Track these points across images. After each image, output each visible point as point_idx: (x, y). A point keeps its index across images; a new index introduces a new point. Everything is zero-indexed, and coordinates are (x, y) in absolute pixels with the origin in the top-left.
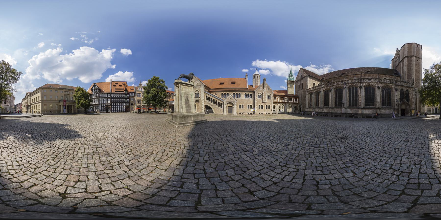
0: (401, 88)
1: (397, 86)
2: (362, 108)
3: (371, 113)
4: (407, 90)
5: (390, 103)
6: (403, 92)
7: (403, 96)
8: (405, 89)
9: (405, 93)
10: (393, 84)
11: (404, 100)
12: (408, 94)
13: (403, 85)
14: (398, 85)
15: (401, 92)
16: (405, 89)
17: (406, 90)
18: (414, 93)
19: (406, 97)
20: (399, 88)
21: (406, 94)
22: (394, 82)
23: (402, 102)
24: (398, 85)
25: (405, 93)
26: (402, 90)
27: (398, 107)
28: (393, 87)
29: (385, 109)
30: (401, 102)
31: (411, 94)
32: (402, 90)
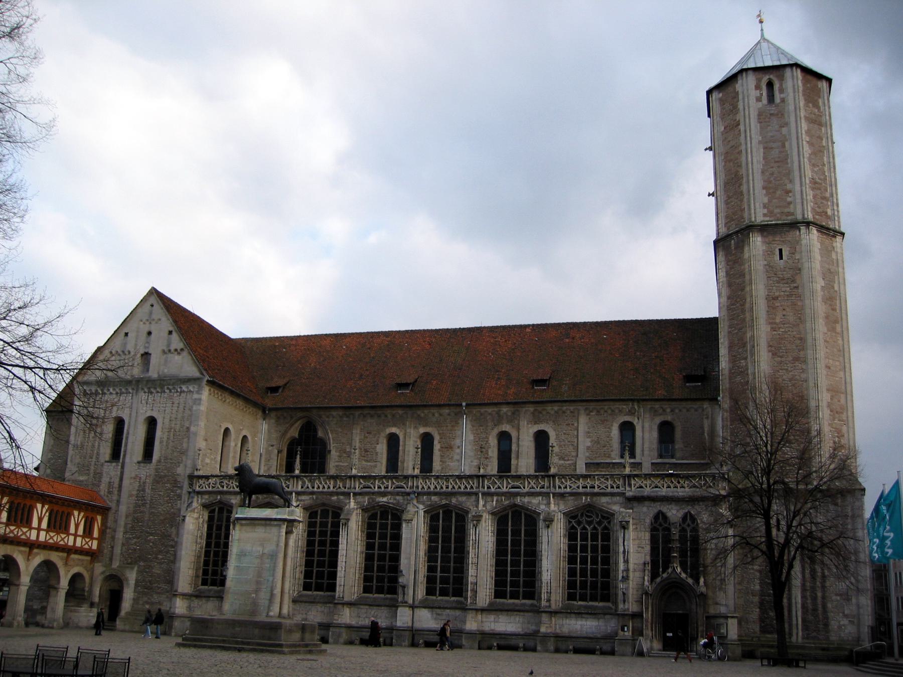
1: (635, 504)
2: (483, 610)
3: (520, 630)
4: (689, 518)
5: (606, 586)
6: (669, 530)
7: (668, 551)
8: (674, 513)
9: (675, 531)
10: (612, 495)
11: (670, 570)
15: (653, 529)
17: (684, 518)
19: (683, 554)
21: (683, 539)
22: (620, 483)
23: (658, 580)
26: (660, 517)
28: (616, 508)
29: (579, 614)
32: (660, 517)
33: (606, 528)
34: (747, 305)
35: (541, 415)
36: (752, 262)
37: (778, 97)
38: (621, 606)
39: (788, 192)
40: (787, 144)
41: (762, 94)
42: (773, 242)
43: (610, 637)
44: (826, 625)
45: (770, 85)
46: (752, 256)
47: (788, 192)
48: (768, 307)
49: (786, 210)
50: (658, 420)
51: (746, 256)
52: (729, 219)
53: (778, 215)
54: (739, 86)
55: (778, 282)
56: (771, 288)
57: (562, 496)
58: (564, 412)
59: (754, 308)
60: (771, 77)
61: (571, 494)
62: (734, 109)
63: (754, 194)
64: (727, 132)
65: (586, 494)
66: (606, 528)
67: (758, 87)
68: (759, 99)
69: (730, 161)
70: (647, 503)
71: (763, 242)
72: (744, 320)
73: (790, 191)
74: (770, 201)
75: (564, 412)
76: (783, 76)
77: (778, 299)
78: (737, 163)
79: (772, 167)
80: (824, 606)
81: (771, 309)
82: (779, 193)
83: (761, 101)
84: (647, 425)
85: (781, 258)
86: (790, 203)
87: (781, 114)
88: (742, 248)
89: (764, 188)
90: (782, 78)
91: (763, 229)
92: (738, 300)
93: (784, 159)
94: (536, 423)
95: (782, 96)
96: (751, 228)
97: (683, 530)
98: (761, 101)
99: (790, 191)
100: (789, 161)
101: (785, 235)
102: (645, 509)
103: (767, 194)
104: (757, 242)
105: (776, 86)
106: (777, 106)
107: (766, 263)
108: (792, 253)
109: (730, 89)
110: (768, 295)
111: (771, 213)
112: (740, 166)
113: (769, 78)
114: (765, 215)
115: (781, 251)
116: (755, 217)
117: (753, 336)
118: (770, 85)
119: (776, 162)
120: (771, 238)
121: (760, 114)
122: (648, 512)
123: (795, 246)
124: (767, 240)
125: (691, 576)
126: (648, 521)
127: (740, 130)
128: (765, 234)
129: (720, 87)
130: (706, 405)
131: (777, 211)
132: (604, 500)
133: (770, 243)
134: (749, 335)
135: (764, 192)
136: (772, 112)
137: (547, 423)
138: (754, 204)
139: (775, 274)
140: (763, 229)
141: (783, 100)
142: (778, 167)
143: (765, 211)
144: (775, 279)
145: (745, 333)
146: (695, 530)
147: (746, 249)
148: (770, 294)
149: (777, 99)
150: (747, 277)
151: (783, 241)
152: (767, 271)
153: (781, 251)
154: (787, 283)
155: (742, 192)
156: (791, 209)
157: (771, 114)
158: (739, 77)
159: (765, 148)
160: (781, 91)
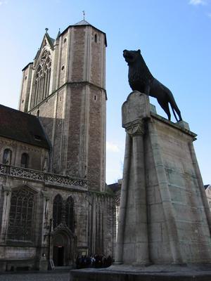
0: (58, 192)
4: (71, 199)
6: (61, 204)
8: (65, 195)
10: (38, 182)
12: (72, 209)
13: (62, 185)
14: (51, 187)
15: (55, 203)
16: (65, 195)
19: (66, 218)
20: (52, 193)
23: (56, 228)
24: (51, 187)
25: (64, 204)
26: (59, 197)
27: (49, 241)
28: (39, 189)
29: (16, 246)
30: (54, 227)
31: (80, 208)
32: (59, 197)
33: (31, 199)
34: (82, 113)
38: (43, 242)
43: (36, 259)
44: (103, 251)
45: (96, 36)
50: (22, 152)
51: (84, 93)
52: (73, 77)
54: (86, 30)
57: (12, 178)
61: (17, 178)
65: (25, 180)
66: (31, 199)
67: (92, 34)
70: (53, 189)
72: (79, 118)
80: (103, 243)
81: (91, 118)
84: (18, 152)
87: (98, 48)
88: (82, 90)
90: (100, 36)
91: (91, 85)
93: (98, 64)
96: (86, 83)
97: (67, 205)
102: (52, 192)
104: (88, 88)
105: (98, 37)
108: (99, 99)
109: (81, 30)
117: (84, 126)
118: (96, 36)
122: (52, 193)
123: (100, 96)
125: (70, 228)
126: (53, 198)
129: (75, 27)
130: (43, 150)
132: (33, 184)
134: (82, 124)
146: (73, 205)
147: (84, 91)
149: (98, 42)
150: (83, 102)
155: (82, 69)
156: (99, 83)
158: (87, 27)
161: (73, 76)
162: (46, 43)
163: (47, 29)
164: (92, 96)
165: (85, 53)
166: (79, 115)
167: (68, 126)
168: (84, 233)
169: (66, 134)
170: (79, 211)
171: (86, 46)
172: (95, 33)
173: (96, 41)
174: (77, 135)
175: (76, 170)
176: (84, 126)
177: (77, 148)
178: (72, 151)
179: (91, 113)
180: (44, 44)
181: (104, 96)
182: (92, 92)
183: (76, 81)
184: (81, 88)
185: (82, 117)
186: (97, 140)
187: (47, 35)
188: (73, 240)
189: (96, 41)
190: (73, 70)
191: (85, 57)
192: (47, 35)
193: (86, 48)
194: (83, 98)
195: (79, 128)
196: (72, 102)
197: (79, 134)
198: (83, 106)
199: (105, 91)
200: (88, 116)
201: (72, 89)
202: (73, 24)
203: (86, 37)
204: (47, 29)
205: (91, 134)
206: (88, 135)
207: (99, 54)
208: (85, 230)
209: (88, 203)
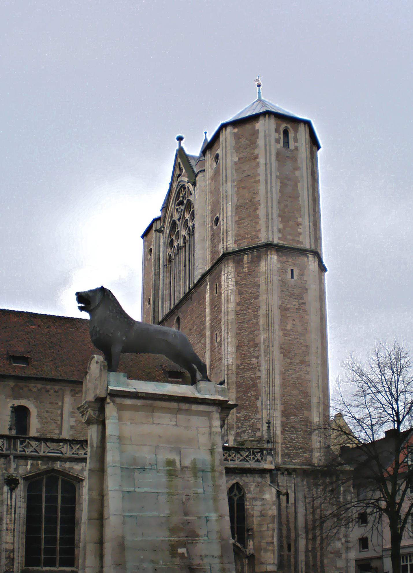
18: (274, 498)
34: (262, 311)
35: (21, 391)
36: (269, 275)
37: (292, 145)
39: (298, 224)
40: (299, 185)
41: (280, 138)
42: (286, 263)
45: (286, 133)
46: (269, 271)
47: (298, 224)
48: (281, 315)
49: (297, 239)
53: (291, 242)
55: (290, 296)
56: (284, 300)
58: (48, 391)
59: (270, 314)
60: (288, 126)
62: (253, 143)
63: (272, 219)
64: (242, 163)
67: (277, 131)
68: (277, 141)
69: (244, 188)
71: (279, 261)
73: (300, 224)
74: (284, 228)
75: (48, 391)
76: (298, 129)
77: (289, 311)
78: (253, 190)
79: (287, 201)
81: (283, 319)
82: (291, 223)
83: (279, 143)
85: (292, 277)
86: (300, 234)
87: (294, 159)
89: (280, 216)
90: (296, 131)
91: (279, 249)
92: (251, 307)
94: (15, 398)
95: (297, 144)
98: (279, 143)
99: (300, 224)
100: (300, 199)
101: (296, 258)
103: (281, 222)
105: (291, 135)
106: (292, 151)
107: (280, 278)
109: (248, 127)
110: (281, 306)
111: (284, 238)
112: (257, 193)
113: (286, 127)
114: (279, 238)
115: (292, 271)
116: (273, 238)
118: (286, 133)
119: (290, 197)
120: (284, 258)
121: (278, 154)
124: (281, 259)
127: (258, 164)
128: (280, 254)
131: (289, 237)
133: (284, 263)
134: (263, 336)
135: (280, 219)
136: (287, 155)
137: (29, 400)
138: (272, 227)
139: (287, 289)
140: (279, 249)
141: (296, 149)
142: (292, 202)
143: (280, 235)
144: (287, 293)
145: (257, 335)
147: (263, 264)
148: (283, 305)
150: (263, 288)
151: (294, 264)
152: (281, 286)
153: (292, 271)
154: (296, 299)
155: (257, 217)
157: (287, 157)
159: (281, 183)
160: (296, 140)
161: (237, 235)
162: (181, 170)
163: (180, 139)
164: (282, 271)
165: (262, 178)
166: (256, 317)
167: (234, 343)
168: (271, 548)
169: (230, 361)
170: (258, 508)
171: (261, 160)
172: (283, 126)
173: (286, 143)
174: (254, 360)
175: (255, 430)
176: (267, 339)
177: (255, 385)
178: (245, 393)
179: (283, 309)
180: (177, 172)
181: (312, 264)
182: (283, 263)
183: (245, 245)
184: (255, 262)
185: (262, 321)
186: (303, 362)
187: (181, 153)
188: (246, 561)
189: (286, 143)
190: (238, 223)
191: (262, 188)
192: (181, 153)
193: (261, 170)
194: (262, 280)
195: (256, 345)
196: (240, 293)
197: (258, 357)
198: (263, 298)
199: (317, 255)
200: (276, 314)
201: (239, 263)
202: (230, 118)
203: (261, 142)
204: (180, 139)
205: (286, 352)
206: (278, 356)
207: (297, 173)
208: (273, 543)
209: (274, 491)
